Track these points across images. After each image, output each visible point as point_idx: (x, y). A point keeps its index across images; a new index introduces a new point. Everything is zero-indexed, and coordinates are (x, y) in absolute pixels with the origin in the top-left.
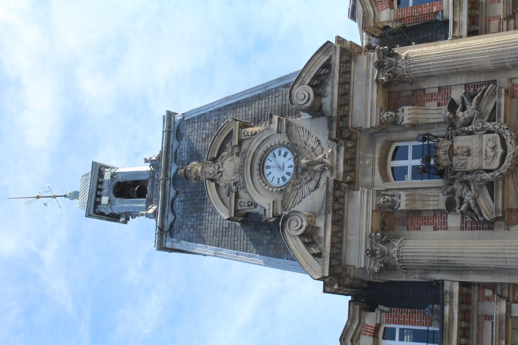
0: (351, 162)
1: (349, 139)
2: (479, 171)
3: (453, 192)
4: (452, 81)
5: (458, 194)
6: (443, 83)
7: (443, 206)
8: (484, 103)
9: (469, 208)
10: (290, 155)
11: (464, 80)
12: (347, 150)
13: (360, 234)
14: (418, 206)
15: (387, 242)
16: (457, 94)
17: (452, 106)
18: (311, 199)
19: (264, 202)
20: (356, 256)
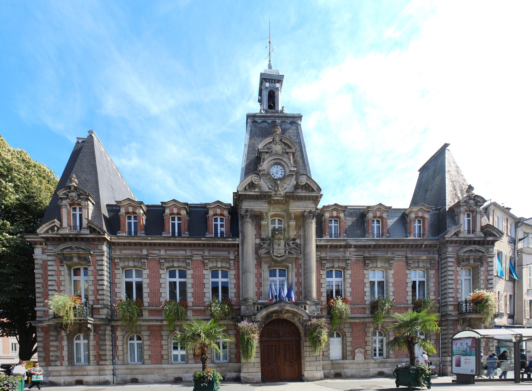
0: (278, 202)
1: (286, 201)
2: (273, 249)
3: (267, 240)
4: (302, 239)
5: (266, 242)
6: (302, 236)
7: (262, 237)
8: (294, 250)
9: (261, 246)
10: (281, 176)
11: (302, 244)
12: (282, 200)
13: (253, 206)
14: (262, 228)
15: (251, 217)
16: (298, 241)
17: (294, 239)
18: (265, 186)
19: (264, 166)
20: (246, 205)
